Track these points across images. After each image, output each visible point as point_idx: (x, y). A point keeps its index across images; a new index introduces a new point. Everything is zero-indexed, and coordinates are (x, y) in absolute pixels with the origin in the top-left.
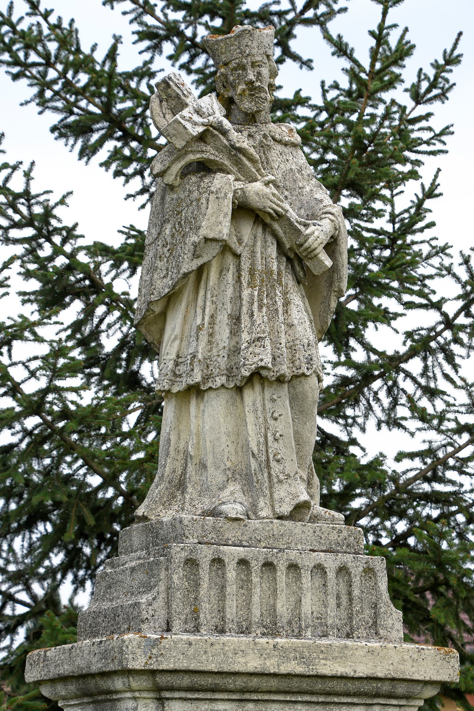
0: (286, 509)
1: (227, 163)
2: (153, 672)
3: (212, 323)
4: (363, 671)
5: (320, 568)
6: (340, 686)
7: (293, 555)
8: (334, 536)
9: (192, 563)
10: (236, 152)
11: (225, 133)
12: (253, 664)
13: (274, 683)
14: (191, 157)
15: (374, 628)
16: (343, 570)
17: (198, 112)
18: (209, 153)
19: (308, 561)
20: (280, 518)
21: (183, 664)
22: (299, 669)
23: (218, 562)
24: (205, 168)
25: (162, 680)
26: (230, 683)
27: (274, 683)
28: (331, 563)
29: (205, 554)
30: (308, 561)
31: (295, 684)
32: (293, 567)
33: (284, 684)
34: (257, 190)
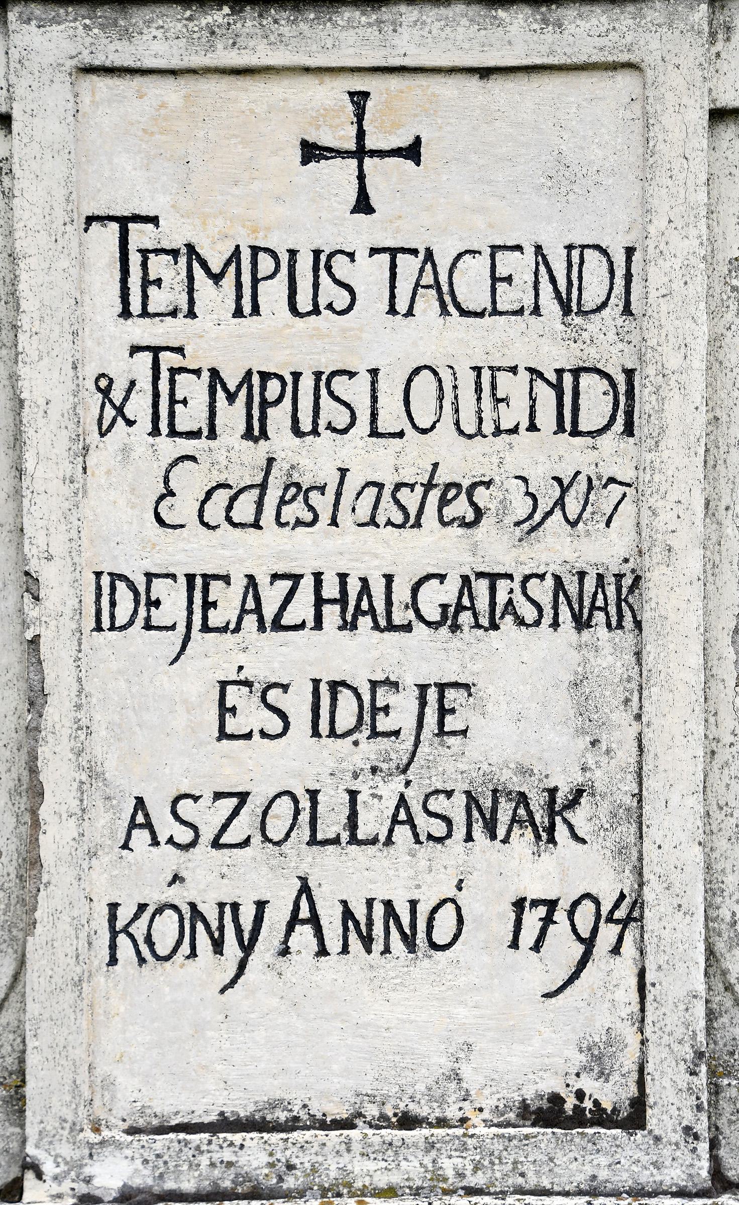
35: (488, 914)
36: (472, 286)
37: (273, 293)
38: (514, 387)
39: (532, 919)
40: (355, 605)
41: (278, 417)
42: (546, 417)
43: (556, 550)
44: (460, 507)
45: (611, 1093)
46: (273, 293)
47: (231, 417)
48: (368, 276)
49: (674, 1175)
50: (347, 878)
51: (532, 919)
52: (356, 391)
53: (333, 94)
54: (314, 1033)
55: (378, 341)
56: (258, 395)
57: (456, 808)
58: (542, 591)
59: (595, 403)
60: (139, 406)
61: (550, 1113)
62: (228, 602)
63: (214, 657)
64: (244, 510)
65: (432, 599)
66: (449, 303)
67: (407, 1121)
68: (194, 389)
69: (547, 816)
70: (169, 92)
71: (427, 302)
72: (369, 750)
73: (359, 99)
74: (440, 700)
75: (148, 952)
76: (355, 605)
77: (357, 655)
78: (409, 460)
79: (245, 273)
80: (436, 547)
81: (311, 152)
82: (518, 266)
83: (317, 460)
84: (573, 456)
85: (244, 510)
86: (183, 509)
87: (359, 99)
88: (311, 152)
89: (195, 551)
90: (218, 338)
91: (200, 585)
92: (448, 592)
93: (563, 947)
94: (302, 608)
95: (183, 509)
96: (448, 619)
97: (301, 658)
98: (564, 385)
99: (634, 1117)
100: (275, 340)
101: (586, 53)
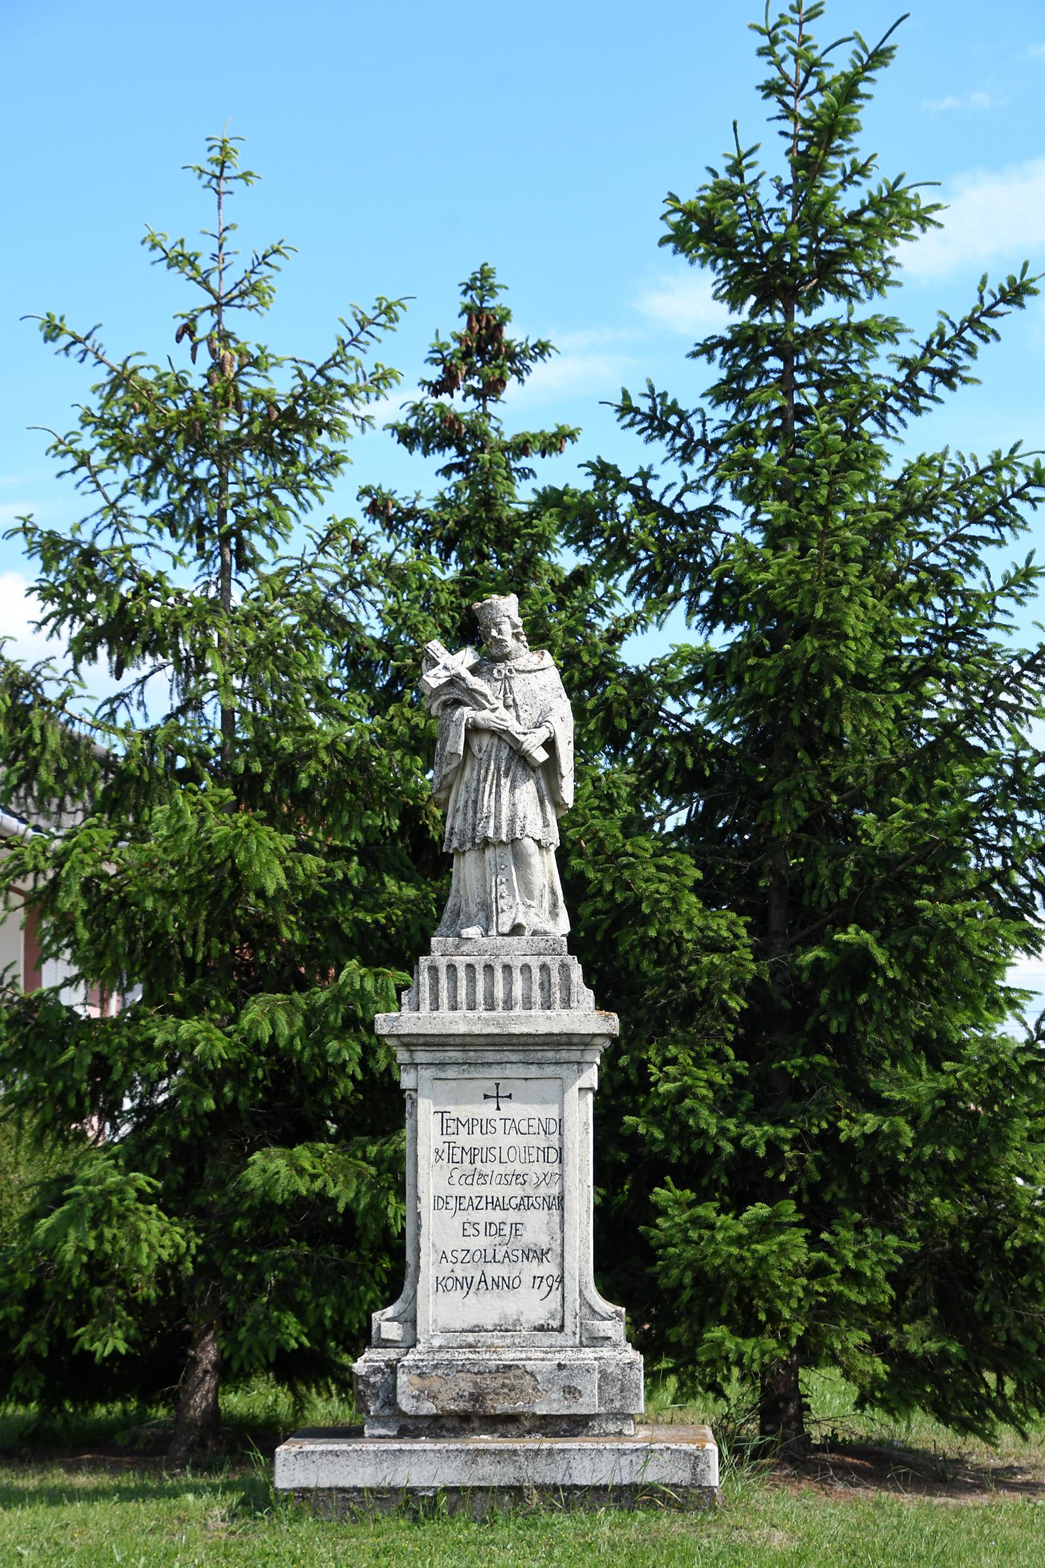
0: (506, 929)
1: (466, 699)
2: (399, 1036)
3: (466, 806)
4: (543, 1030)
5: (526, 968)
6: (530, 1040)
7: (507, 960)
8: (542, 944)
9: (433, 969)
10: (471, 692)
11: (464, 680)
12: (462, 1029)
13: (482, 1040)
14: (443, 698)
15: (567, 1003)
16: (544, 968)
17: (445, 668)
18: (456, 694)
19: (517, 962)
20: (503, 935)
21: (415, 1031)
22: (496, 1031)
23: (451, 968)
24: (458, 703)
25: (406, 1040)
26: (451, 1040)
27: (482, 1040)
28: (535, 962)
29: (442, 963)
30: (517, 962)
31: (497, 1040)
32: (507, 968)
33: (489, 1040)
34: (483, 717)
35: (527, 1280)
36: (524, 1129)
37: (477, 1129)
38: (533, 1151)
39: (538, 1281)
40: (495, 1204)
41: (478, 1158)
42: (541, 1159)
43: (543, 1191)
44: (521, 1180)
45: (555, 1324)
46: (477, 1129)
47: (467, 1158)
48: (499, 1125)
49: (570, 1343)
50: (493, 1271)
51: (538, 1281)
52: (496, 1152)
53: (492, 1084)
54: (484, 1309)
55: (503, 1140)
56: (473, 1153)
57: (519, 1254)
58: (540, 1200)
59: (553, 1155)
60: (445, 1156)
61: (541, 1329)
62: (465, 1203)
63: (461, 1217)
64: (469, 1181)
65: (514, 1202)
66: (518, 1131)
67: (507, 1330)
68: (458, 1152)
69: (541, 1255)
70: (453, 1083)
71: (513, 1131)
72: (498, 1239)
73: (497, 1085)
74: (515, 1226)
75: (446, 1289)
76: (495, 1204)
77: (497, 1216)
78: (509, 1168)
79: (470, 1124)
80: (516, 1190)
81: (486, 1097)
82: (535, 1123)
83: (487, 1168)
84: (548, 1168)
85: (469, 1181)
86: (455, 1180)
87: (497, 1085)
88: (486, 1097)
89: (458, 1190)
90: (464, 1139)
91: (459, 1199)
92: (518, 1201)
93: (545, 1288)
94: (482, 1205)
95: (455, 1180)
96: (518, 1207)
97: (482, 1217)
98: (545, 1151)
99: (561, 1328)
100: (477, 1140)
101: (550, 1074)
